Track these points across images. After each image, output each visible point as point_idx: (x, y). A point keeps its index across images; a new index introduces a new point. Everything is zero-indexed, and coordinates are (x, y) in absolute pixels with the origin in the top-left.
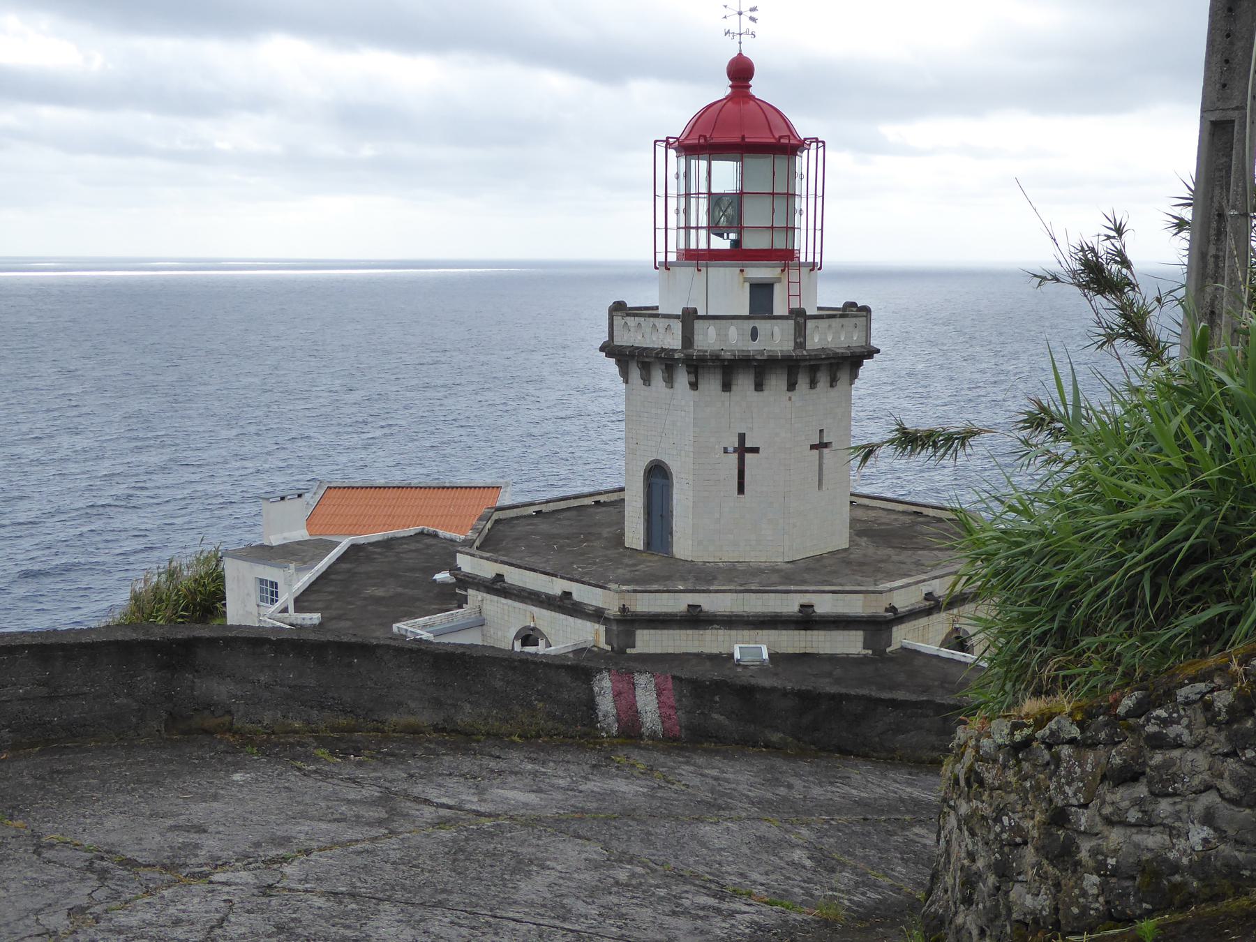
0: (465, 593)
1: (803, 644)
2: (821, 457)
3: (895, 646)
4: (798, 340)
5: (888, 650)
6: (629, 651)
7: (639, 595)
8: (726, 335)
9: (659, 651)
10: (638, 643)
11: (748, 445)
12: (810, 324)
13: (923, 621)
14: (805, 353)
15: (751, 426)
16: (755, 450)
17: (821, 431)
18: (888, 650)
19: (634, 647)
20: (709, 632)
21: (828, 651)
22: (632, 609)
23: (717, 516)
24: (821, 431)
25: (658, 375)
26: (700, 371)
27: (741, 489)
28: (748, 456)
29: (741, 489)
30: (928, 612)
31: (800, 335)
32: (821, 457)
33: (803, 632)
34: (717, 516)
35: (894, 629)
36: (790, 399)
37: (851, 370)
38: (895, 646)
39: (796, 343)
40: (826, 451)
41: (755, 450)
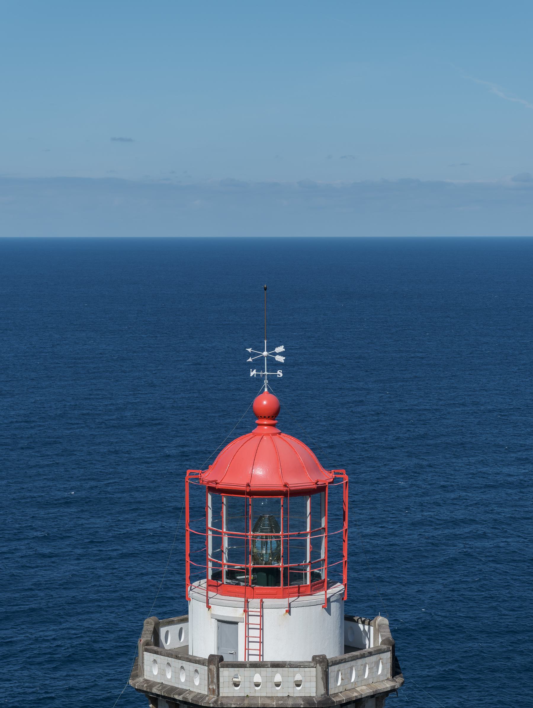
4: (211, 687)
31: (212, 682)
39: (209, 689)
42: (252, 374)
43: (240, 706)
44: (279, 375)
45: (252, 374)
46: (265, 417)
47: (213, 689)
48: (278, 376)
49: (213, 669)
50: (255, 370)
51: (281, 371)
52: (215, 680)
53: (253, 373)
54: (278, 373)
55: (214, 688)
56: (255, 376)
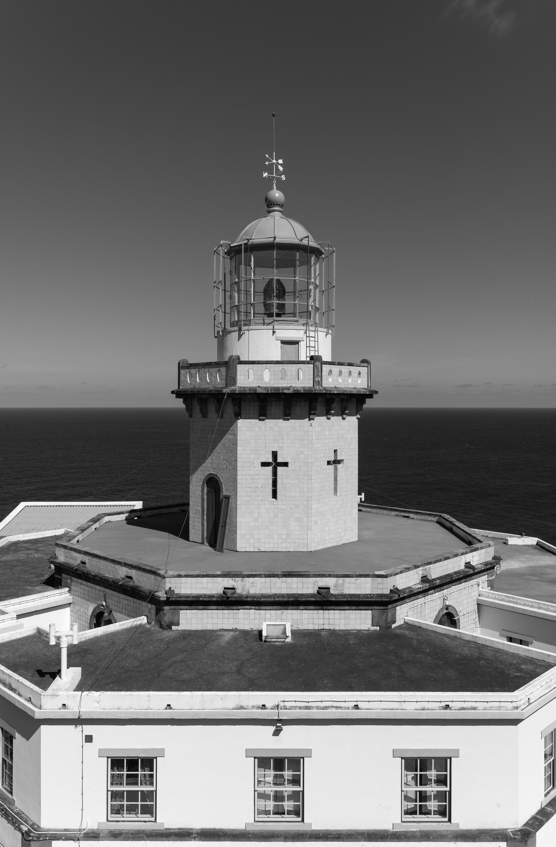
0: (59, 577)
1: (321, 622)
2: (336, 470)
3: (399, 622)
4: (316, 379)
5: (394, 626)
6: (174, 628)
7: (183, 580)
8: (262, 376)
9: (199, 628)
10: (181, 621)
11: (280, 460)
12: (326, 368)
13: (420, 601)
14: (321, 388)
15: (281, 445)
16: (285, 464)
17: (335, 451)
18: (394, 626)
19: (178, 624)
20: (241, 611)
21: (343, 628)
22: (177, 591)
23: (256, 515)
24: (335, 451)
25: (212, 408)
26: (243, 404)
27: (275, 495)
28: (279, 469)
29: (275, 495)
30: (424, 592)
32: (336, 470)
33: (321, 612)
34: (256, 515)
35: (398, 608)
36: (311, 425)
37: (357, 406)
38: (399, 622)
40: (339, 466)
41: (285, 464)
42: (264, 175)
43: (339, 393)
44: (283, 179)
45: (264, 175)
46: (277, 205)
47: (318, 381)
48: (282, 179)
49: (318, 365)
50: (267, 173)
51: (284, 176)
52: (320, 374)
53: (265, 175)
54: (283, 176)
55: (319, 380)
56: (267, 177)
